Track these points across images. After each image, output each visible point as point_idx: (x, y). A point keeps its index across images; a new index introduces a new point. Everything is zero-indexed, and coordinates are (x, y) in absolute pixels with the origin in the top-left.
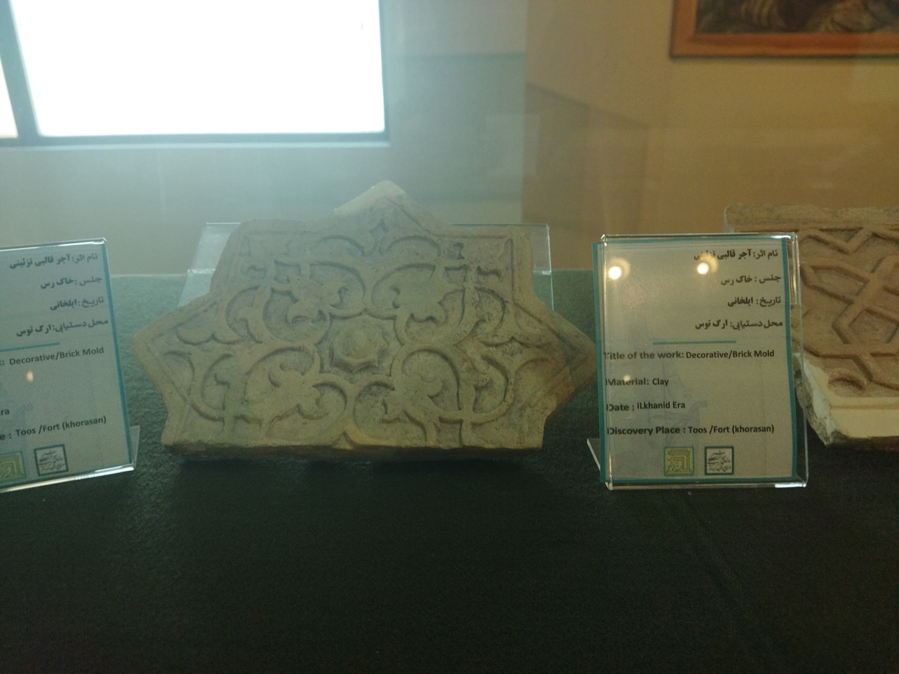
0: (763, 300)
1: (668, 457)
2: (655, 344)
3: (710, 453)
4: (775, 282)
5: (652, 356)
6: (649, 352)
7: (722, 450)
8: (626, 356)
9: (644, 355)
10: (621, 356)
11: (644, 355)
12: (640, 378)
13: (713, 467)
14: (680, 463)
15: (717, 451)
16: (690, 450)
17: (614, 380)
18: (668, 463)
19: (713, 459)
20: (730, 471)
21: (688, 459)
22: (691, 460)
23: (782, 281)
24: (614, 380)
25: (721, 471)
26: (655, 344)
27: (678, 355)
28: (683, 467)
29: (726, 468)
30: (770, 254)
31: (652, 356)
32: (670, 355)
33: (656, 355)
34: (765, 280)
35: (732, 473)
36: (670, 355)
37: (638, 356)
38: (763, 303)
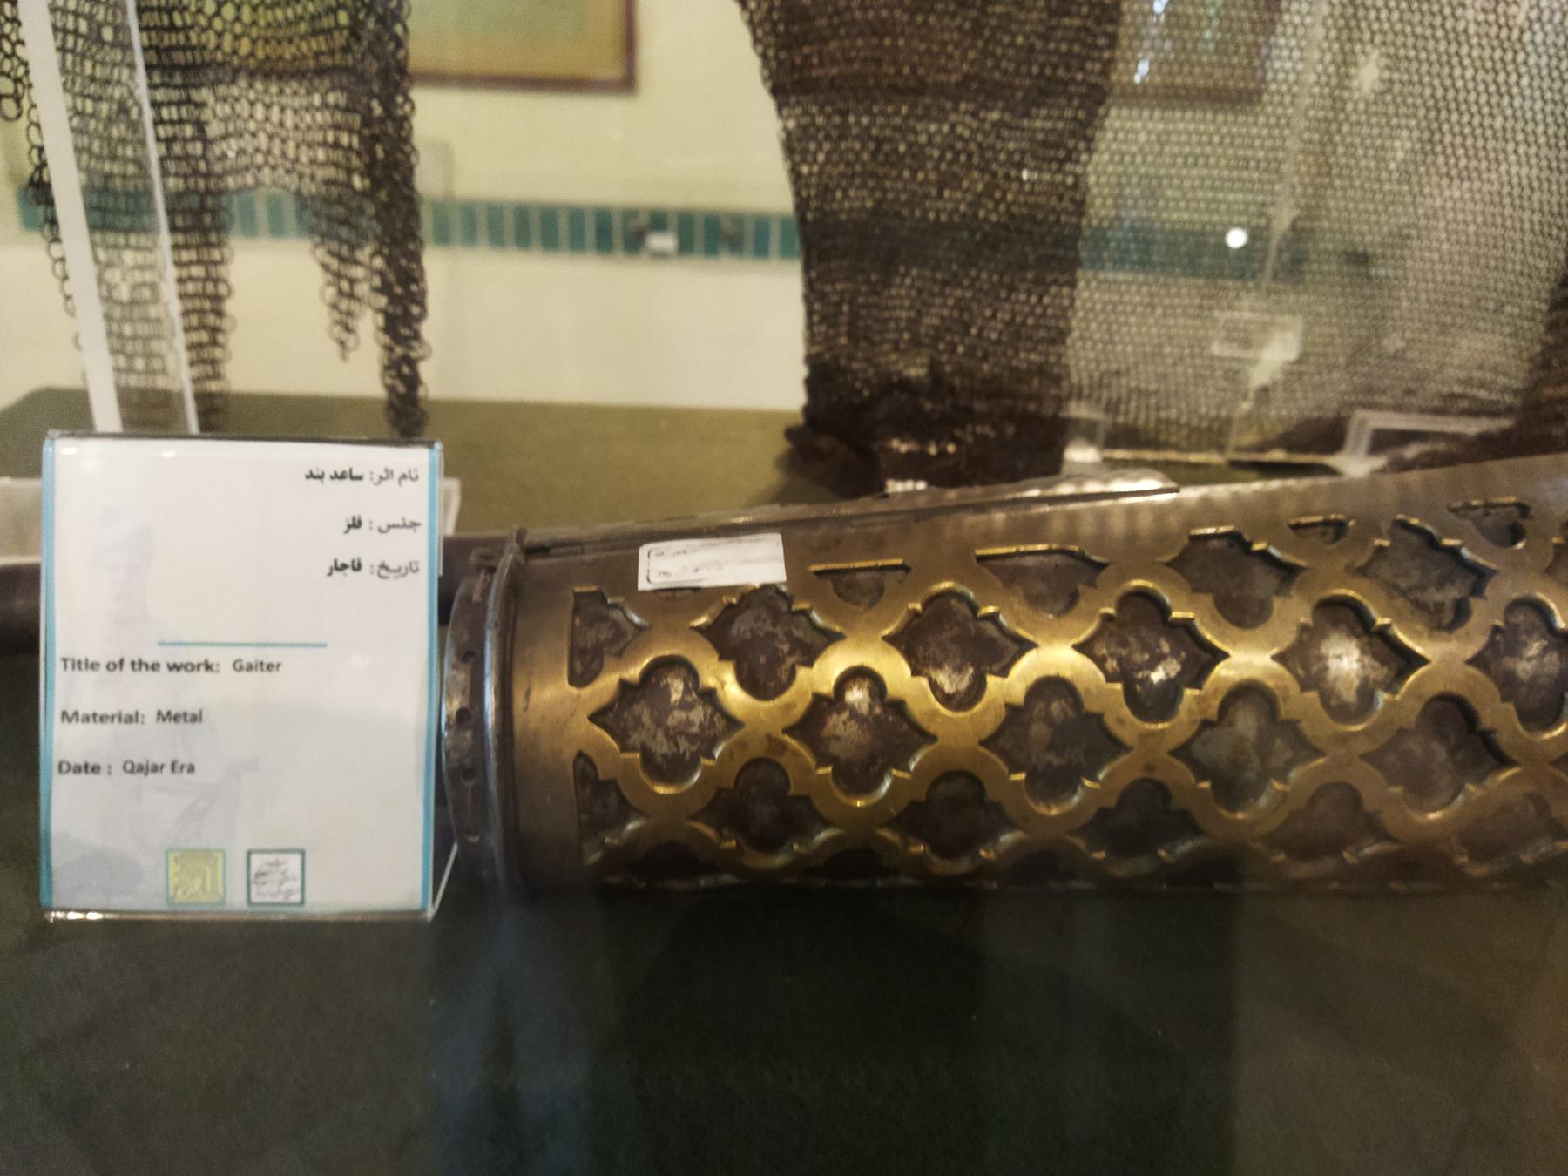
0: (383, 566)
1: (174, 868)
2: (161, 644)
3: (258, 862)
4: (409, 532)
5: (154, 667)
6: (150, 660)
7: (282, 857)
8: (103, 667)
9: (138, 665)
10: (94, 666)
11: (138, 665)
12: (129, 710)
13: (265, 889)
14: (198, 882)
15: (272, 858)
16: (220, 856)
17: (76, 714)
18: (173, 881)
19: (263, 874)
20: (296, 898)
21: (214, 875)
22: (220, 873)
23: (423, 531)
24: (76, 714)
25: (280, 899)
26: (161, 644)
27: (208, 667)
28: (203, 887)
29: (289, 892)
30: (404, 477)
31: (154, 667)
32: (195, 667)
33: (164, 668)
34: (389, 527)
35: (302, 903)
36: (195, 667)
37: (127, 665)
38: (383, 572)
